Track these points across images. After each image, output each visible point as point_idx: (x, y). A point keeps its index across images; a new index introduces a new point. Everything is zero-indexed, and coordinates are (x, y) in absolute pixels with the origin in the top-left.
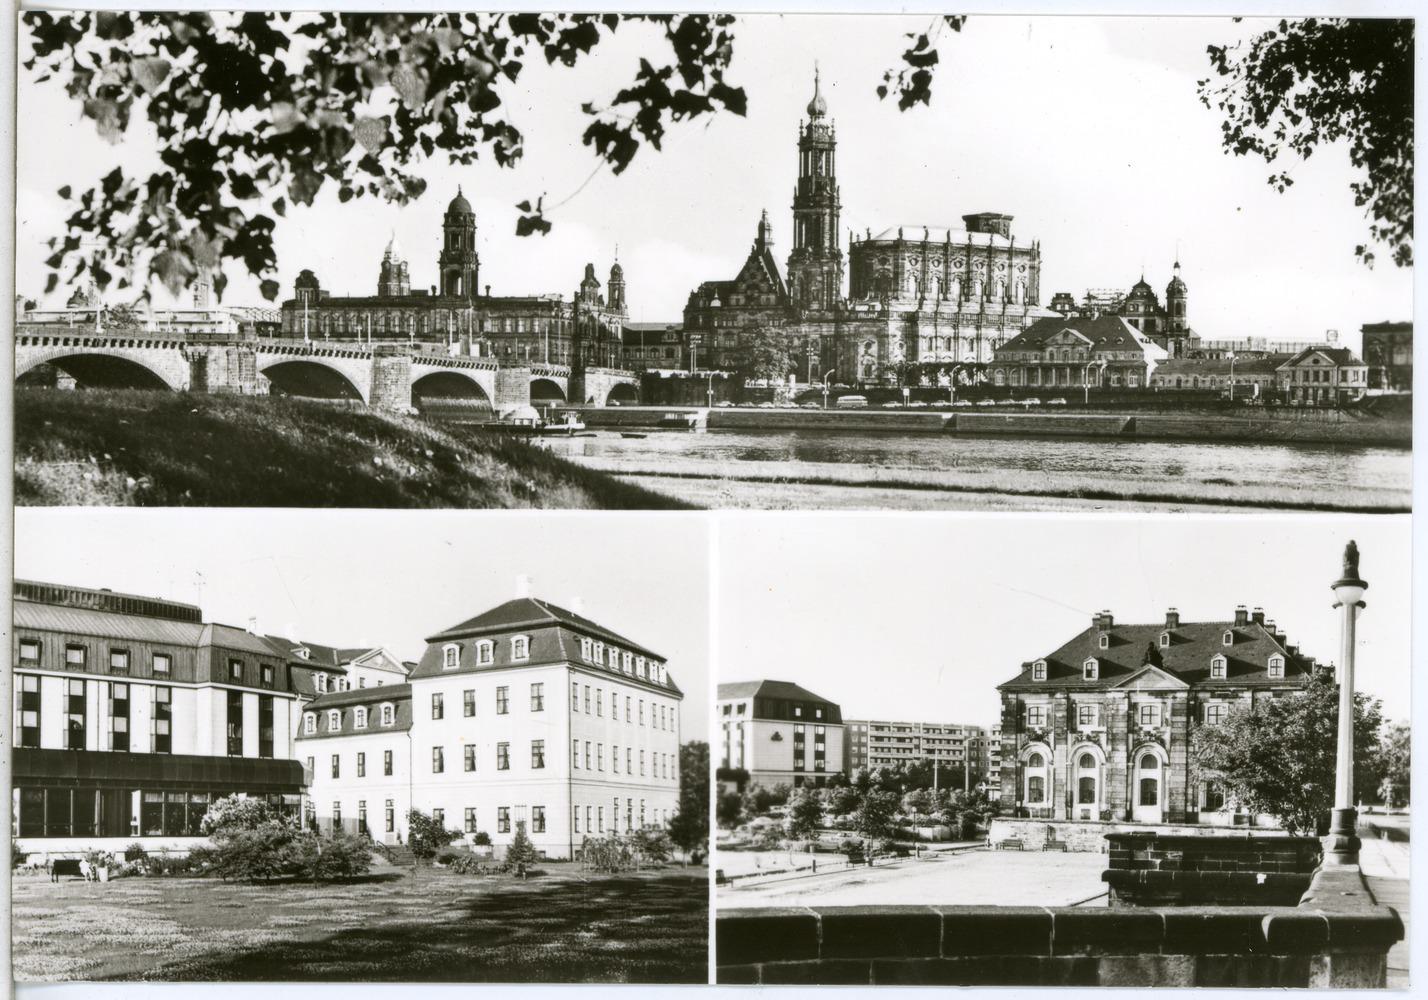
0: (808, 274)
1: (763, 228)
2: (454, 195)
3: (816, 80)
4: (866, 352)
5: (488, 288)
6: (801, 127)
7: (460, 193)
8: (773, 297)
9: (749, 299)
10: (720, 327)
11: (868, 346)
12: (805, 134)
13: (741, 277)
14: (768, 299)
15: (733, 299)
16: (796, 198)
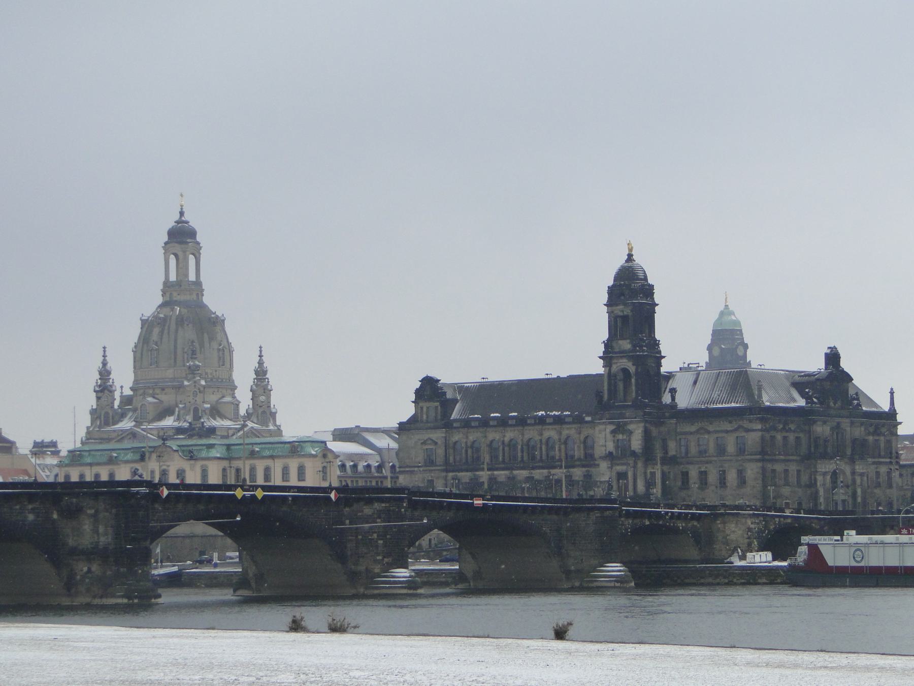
7: (630, 258)
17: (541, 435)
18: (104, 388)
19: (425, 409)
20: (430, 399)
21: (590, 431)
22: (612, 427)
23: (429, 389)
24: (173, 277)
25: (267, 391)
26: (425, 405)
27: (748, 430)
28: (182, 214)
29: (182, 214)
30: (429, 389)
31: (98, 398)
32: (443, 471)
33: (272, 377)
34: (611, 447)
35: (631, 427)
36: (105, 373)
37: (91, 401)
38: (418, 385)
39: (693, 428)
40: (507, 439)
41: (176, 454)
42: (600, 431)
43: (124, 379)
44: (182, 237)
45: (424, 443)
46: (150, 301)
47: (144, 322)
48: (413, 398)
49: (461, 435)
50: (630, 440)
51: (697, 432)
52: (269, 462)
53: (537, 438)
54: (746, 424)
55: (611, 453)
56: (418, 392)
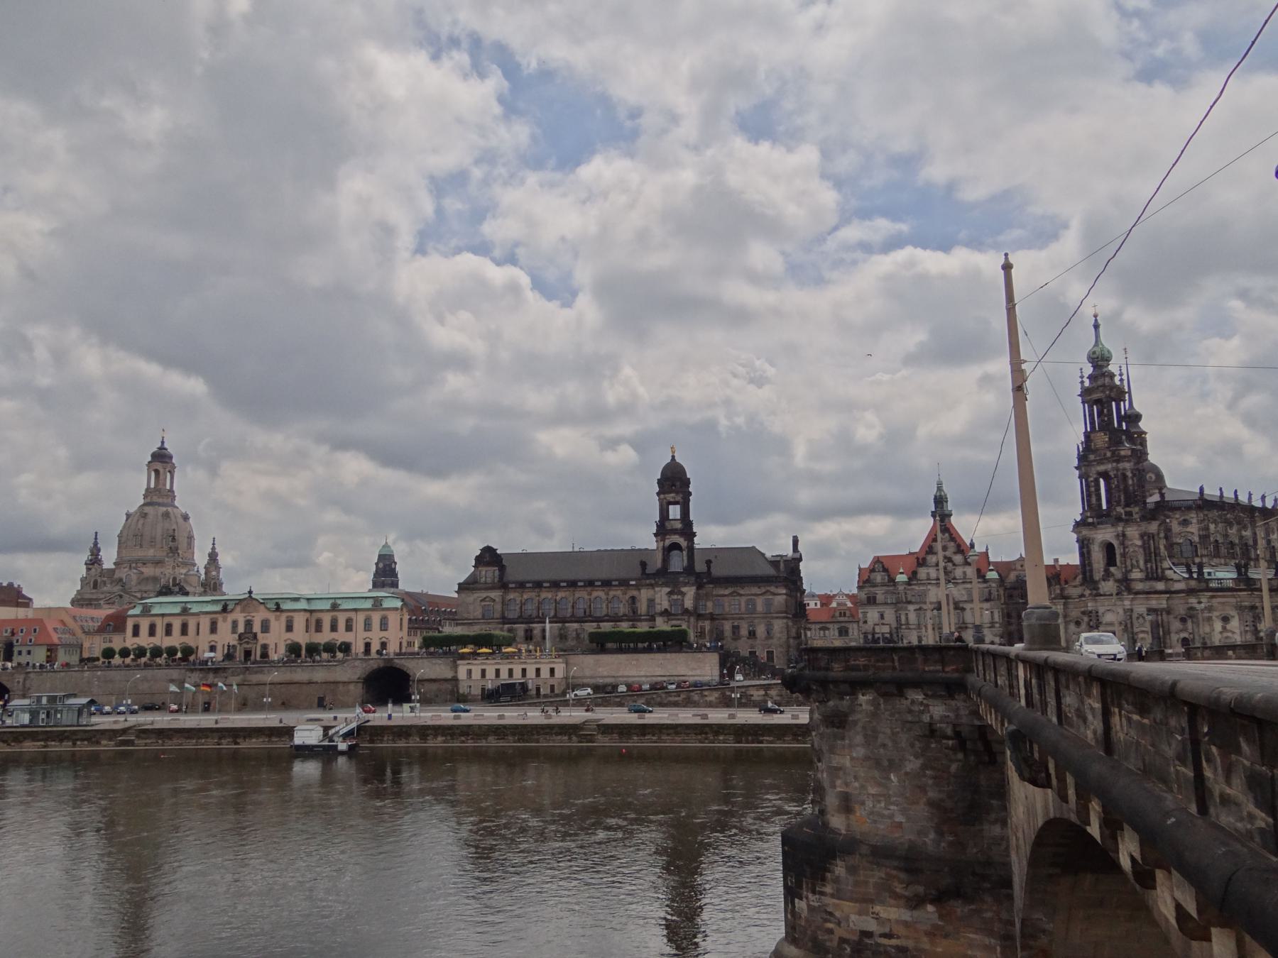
0: (1124, 535)
1: (940, 501)
2: (669, 460)
3: (1096, 326)
4: (1224, 628)
5: (709, 562)
6: (1082, 377)
8: (970, 572)
9: (946, 572)
10: (910, 603)
11: (1226, 619)
12: (1087, 383)
13: (929, 549)
14: (965, 573)
15: (922, 573)
16: (1083, 458)
18: (94, 560)
20: (488, 564)
21: (635, 593)
22: (668, 590)
24: (152, 485)
27: (775, 594)
28: (163, 443)
29: (163, 443)
30: (488, 557)
31: (88, 569)
33: (224, 560)
34: (665, 605)
35: (684, 589)
36: (95, 551)
37: (83, 571)
39: (727, 592)
41: (262, 607)
43: (109, 558)
44: (161, 458)
46: (137, 501)
47: (128, 516)
51: (731, 594)
52: (352, 615)
53: (587, 597)
54: (773, 589)
56: (478, 559)
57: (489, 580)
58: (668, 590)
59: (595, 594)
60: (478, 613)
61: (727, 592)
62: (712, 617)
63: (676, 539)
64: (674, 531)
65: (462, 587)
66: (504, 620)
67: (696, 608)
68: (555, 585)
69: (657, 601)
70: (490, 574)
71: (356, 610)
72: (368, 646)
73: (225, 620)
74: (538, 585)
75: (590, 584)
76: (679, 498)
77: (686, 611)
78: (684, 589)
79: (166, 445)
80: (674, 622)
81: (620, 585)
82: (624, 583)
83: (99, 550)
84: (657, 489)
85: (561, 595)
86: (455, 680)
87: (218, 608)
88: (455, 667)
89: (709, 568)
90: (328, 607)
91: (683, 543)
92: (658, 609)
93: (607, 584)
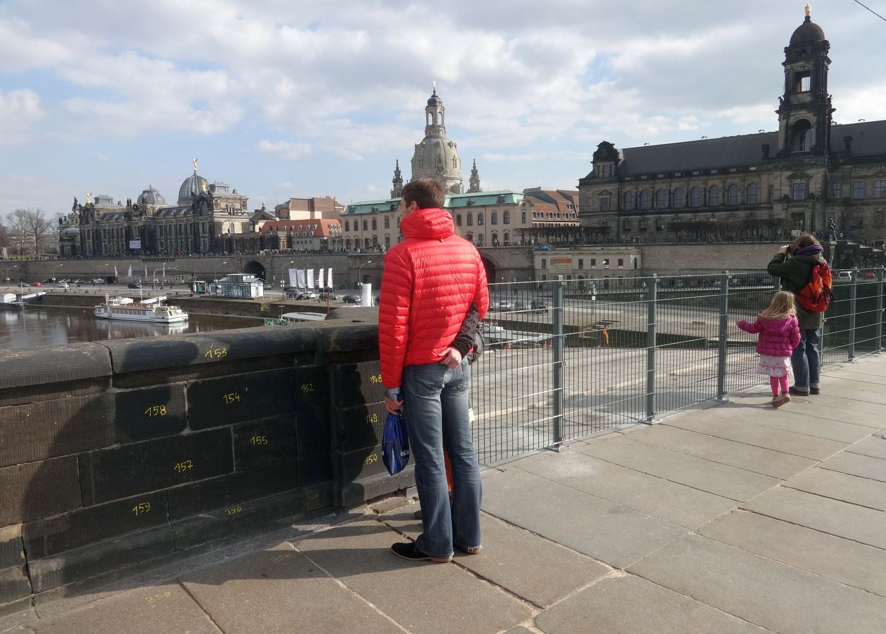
2: (800, 22)
7: (808, 18)
17: (706, 184)
18: (397, 180)
19: (601, 168)
20: (604, 159)
21: (755, 180)
22: (789, 173)
23: (605, 152)
25: (477, 181)
26: (601, 164)
30: (605, 152)
32: (615, 215)
34: (786, 190)
35: (809, 172)
36: (398, 172)
38: (596, 149)
39: (870, 173)
40: (673, 189)
42: (775, 178)
44: (433, 103)
45: (601, 193)
47: (416, 146)
48: (592, 159)
49: (632, 187)
50: (808, 184)
52: (482, 210)
53: (702, 186)
55: (786, 196)
56: (596, 155)
57: (606, 175)
58: (789, 173)
59: (710, 183)
60: (597, 207)
61: (870, 173)
62: (847, 202)
63: (804, 114)
64: (802, 106)
65: (583, 183)
66: (621, 212)
67: (825, 191)
68: (670, 176)
69: (776, 186)
70: (607, 169)
71: (484, 206)
72: (495, 236)
73: (393, 217)
74: (653, 177)
75: (707, 172)
76: (809, 66)
77: (811, 196)
78: (809, 172)
79: (437, 94)
80: (795, 210)
81: (738, 172)
82: (743, 170)
83: (400, 172)
84: (784, 59)
85: (675, 185)
86: (532, 269)
87: (388, 208)
88: (531, 256)
89: (848, 147)
90: (465, 204)
91: (812, 118)
92: (777, 195)
93: (724, 171)
